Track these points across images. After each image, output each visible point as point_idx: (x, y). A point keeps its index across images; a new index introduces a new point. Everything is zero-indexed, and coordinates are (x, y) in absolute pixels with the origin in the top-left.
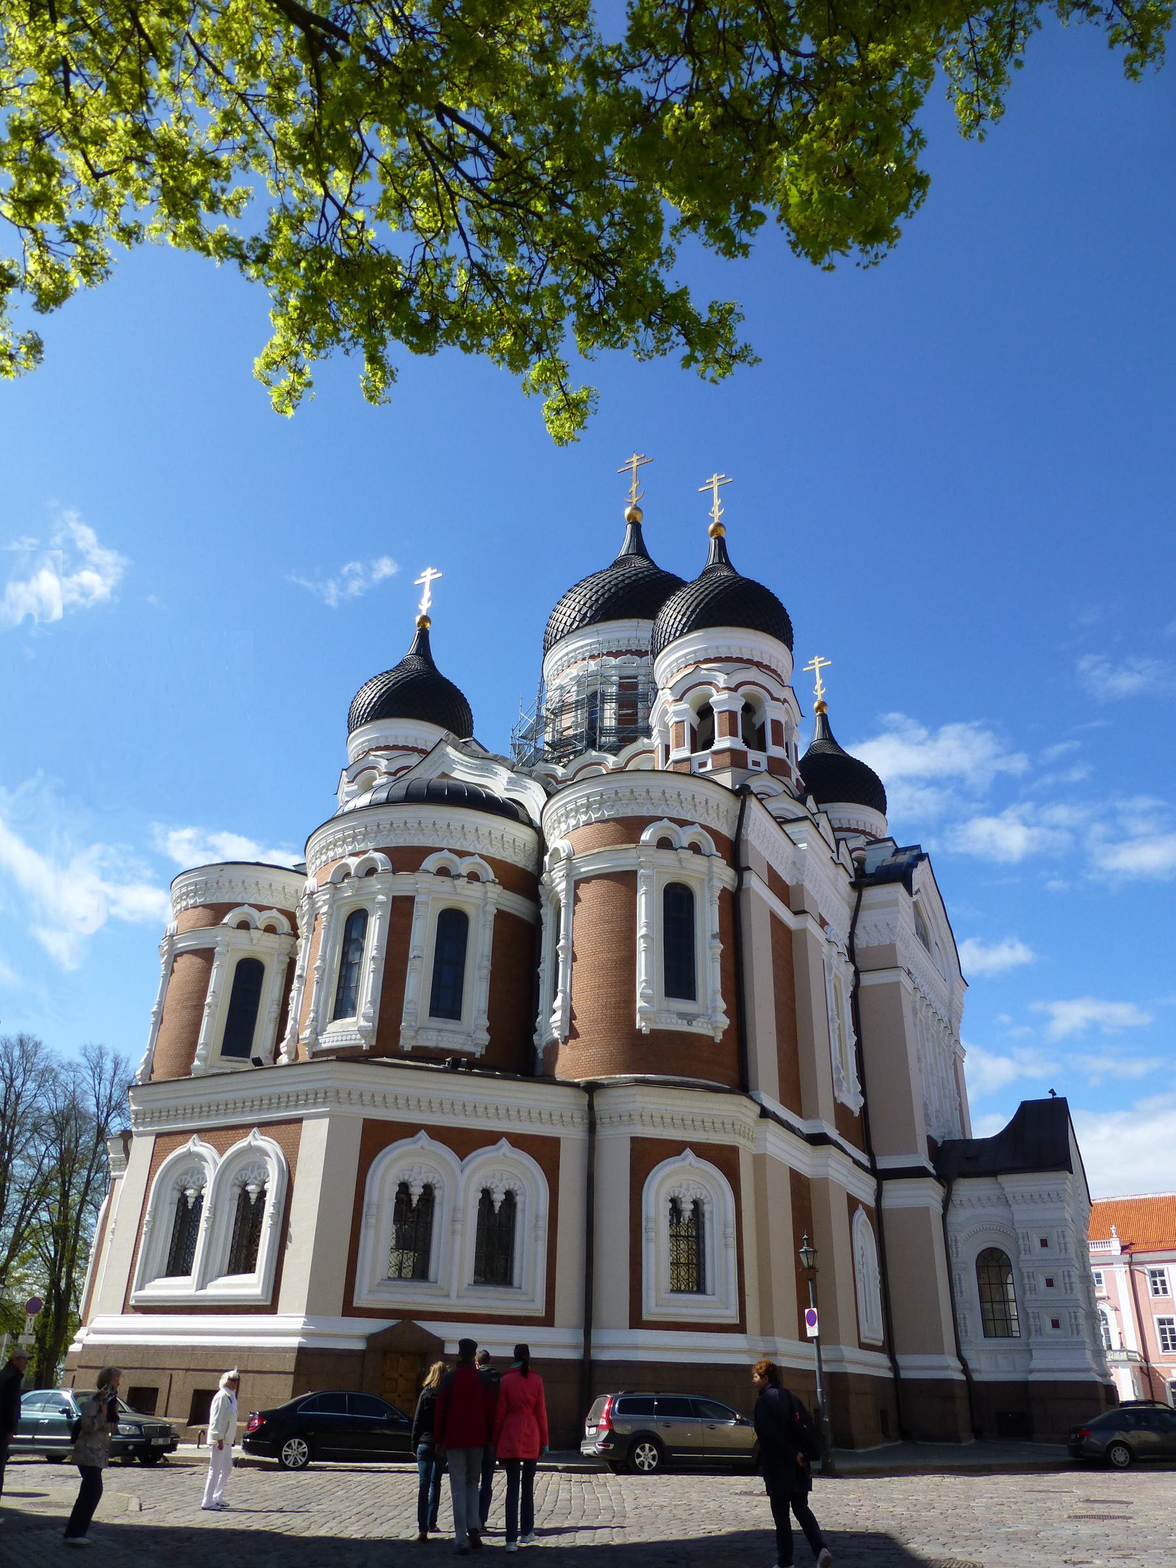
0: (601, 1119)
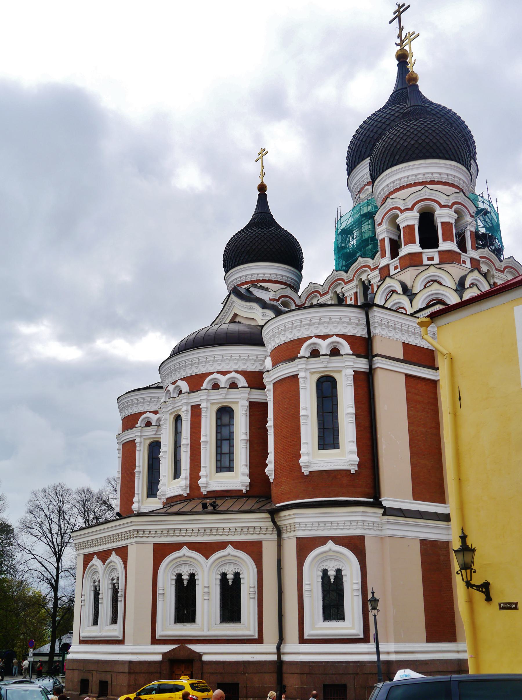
0: (283, 528)
